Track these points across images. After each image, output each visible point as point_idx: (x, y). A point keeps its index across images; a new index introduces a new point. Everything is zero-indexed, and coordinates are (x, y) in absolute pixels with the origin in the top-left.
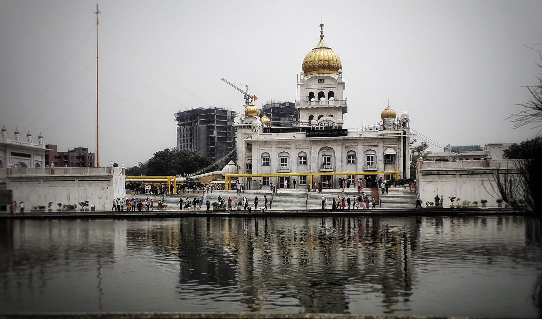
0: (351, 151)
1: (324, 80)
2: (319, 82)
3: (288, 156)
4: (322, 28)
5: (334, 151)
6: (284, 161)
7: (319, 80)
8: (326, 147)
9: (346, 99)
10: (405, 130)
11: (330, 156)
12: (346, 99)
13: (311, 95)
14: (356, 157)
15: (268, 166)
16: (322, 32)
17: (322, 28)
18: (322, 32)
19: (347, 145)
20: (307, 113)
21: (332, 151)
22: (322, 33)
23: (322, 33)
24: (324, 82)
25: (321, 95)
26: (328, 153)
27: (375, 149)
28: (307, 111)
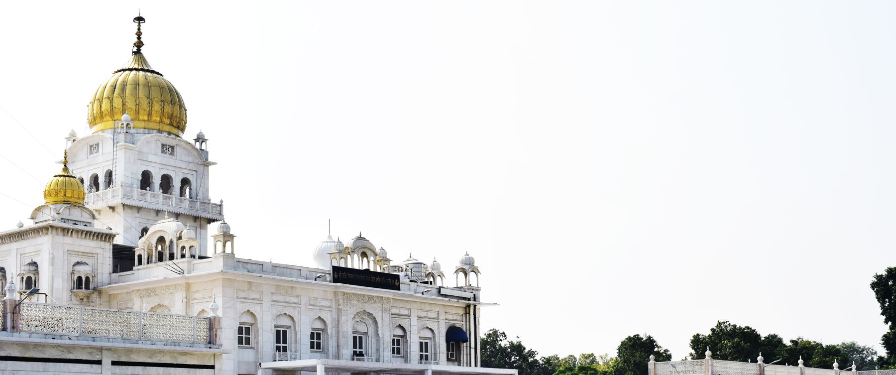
0: (400, 326)
1: (172, 147)
2: (163, 152)
3: (289, 327)
4: (139, 29)
5: (376, 322)
6: (281, 336)
7: (163, 145)
8: (365, 312)
9: (222, 202)
10: (475, 292)
11: (366, 334)
12: (222, 202)
13: (146, 180)
14: (406, 342)
15: (250, 350)
16: (139, 34)
17: (139, 29)
18: (139, 34)
19: (393, 311)
20: (138, 220)
21: (370, 322)
22: (139, 38)
23: (139, 38)
24: (172, 154)
25: (166, 183)
26: (362, 328)
27: (434, 326)
28: (137, 215)
